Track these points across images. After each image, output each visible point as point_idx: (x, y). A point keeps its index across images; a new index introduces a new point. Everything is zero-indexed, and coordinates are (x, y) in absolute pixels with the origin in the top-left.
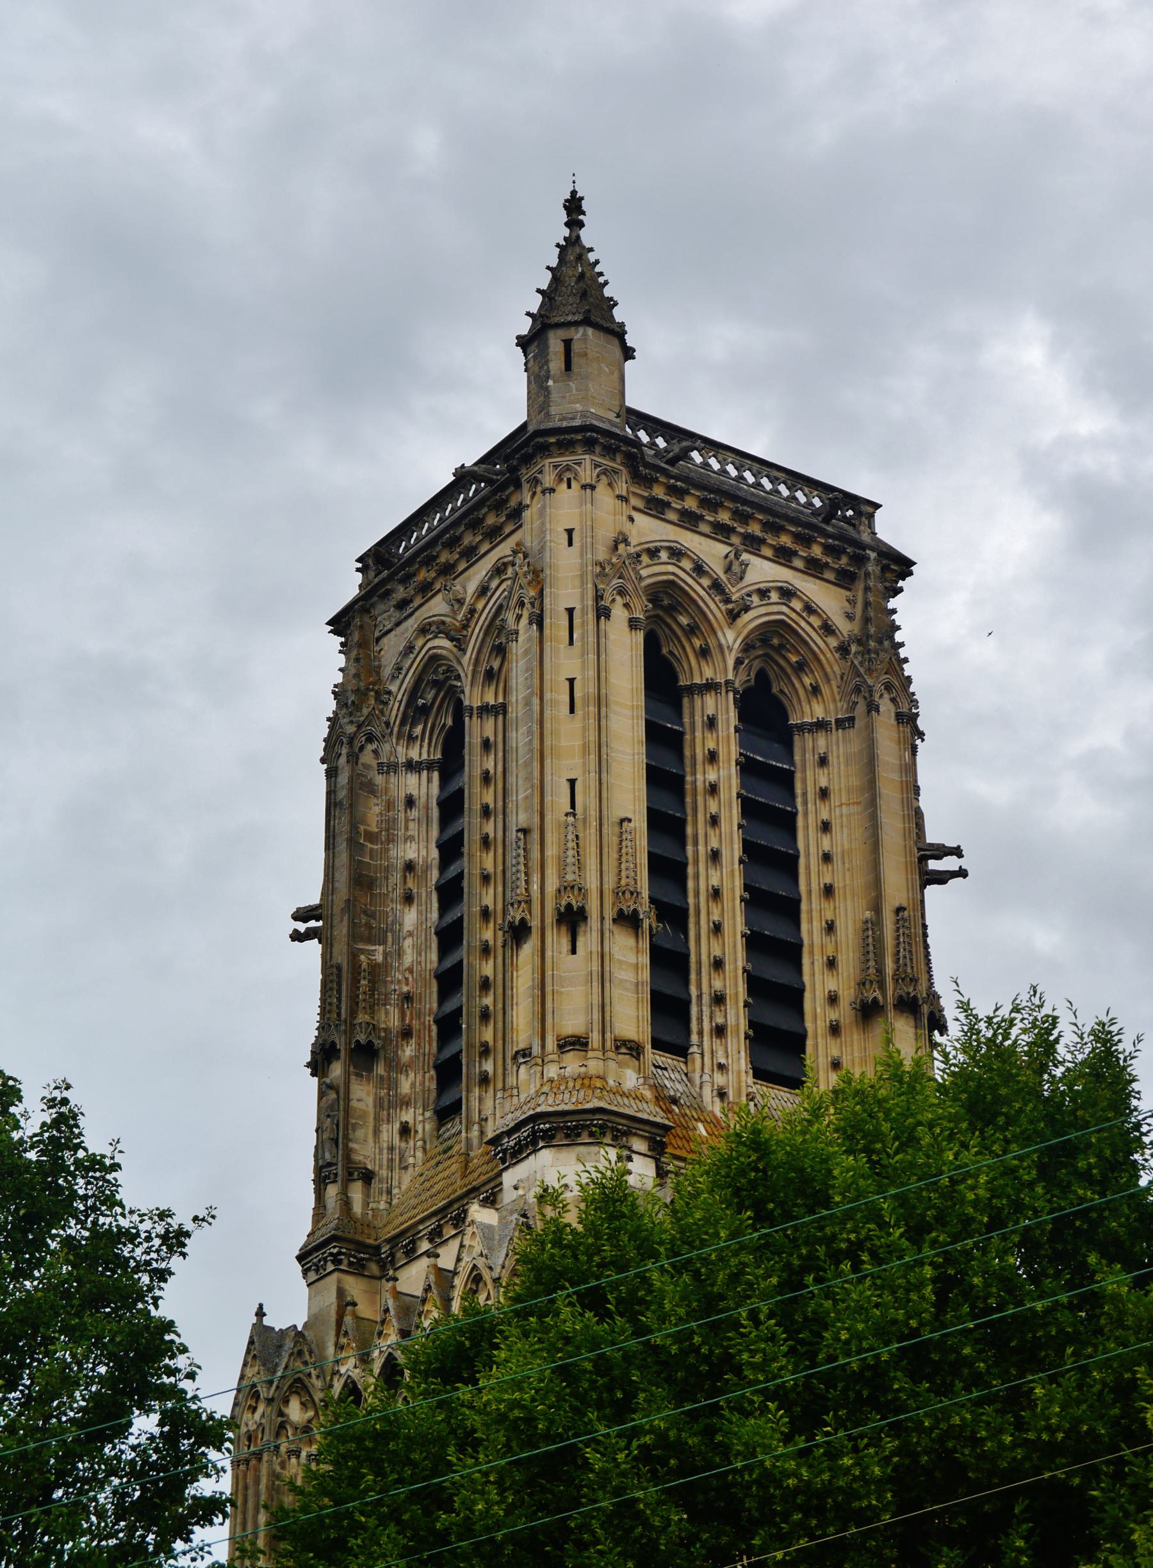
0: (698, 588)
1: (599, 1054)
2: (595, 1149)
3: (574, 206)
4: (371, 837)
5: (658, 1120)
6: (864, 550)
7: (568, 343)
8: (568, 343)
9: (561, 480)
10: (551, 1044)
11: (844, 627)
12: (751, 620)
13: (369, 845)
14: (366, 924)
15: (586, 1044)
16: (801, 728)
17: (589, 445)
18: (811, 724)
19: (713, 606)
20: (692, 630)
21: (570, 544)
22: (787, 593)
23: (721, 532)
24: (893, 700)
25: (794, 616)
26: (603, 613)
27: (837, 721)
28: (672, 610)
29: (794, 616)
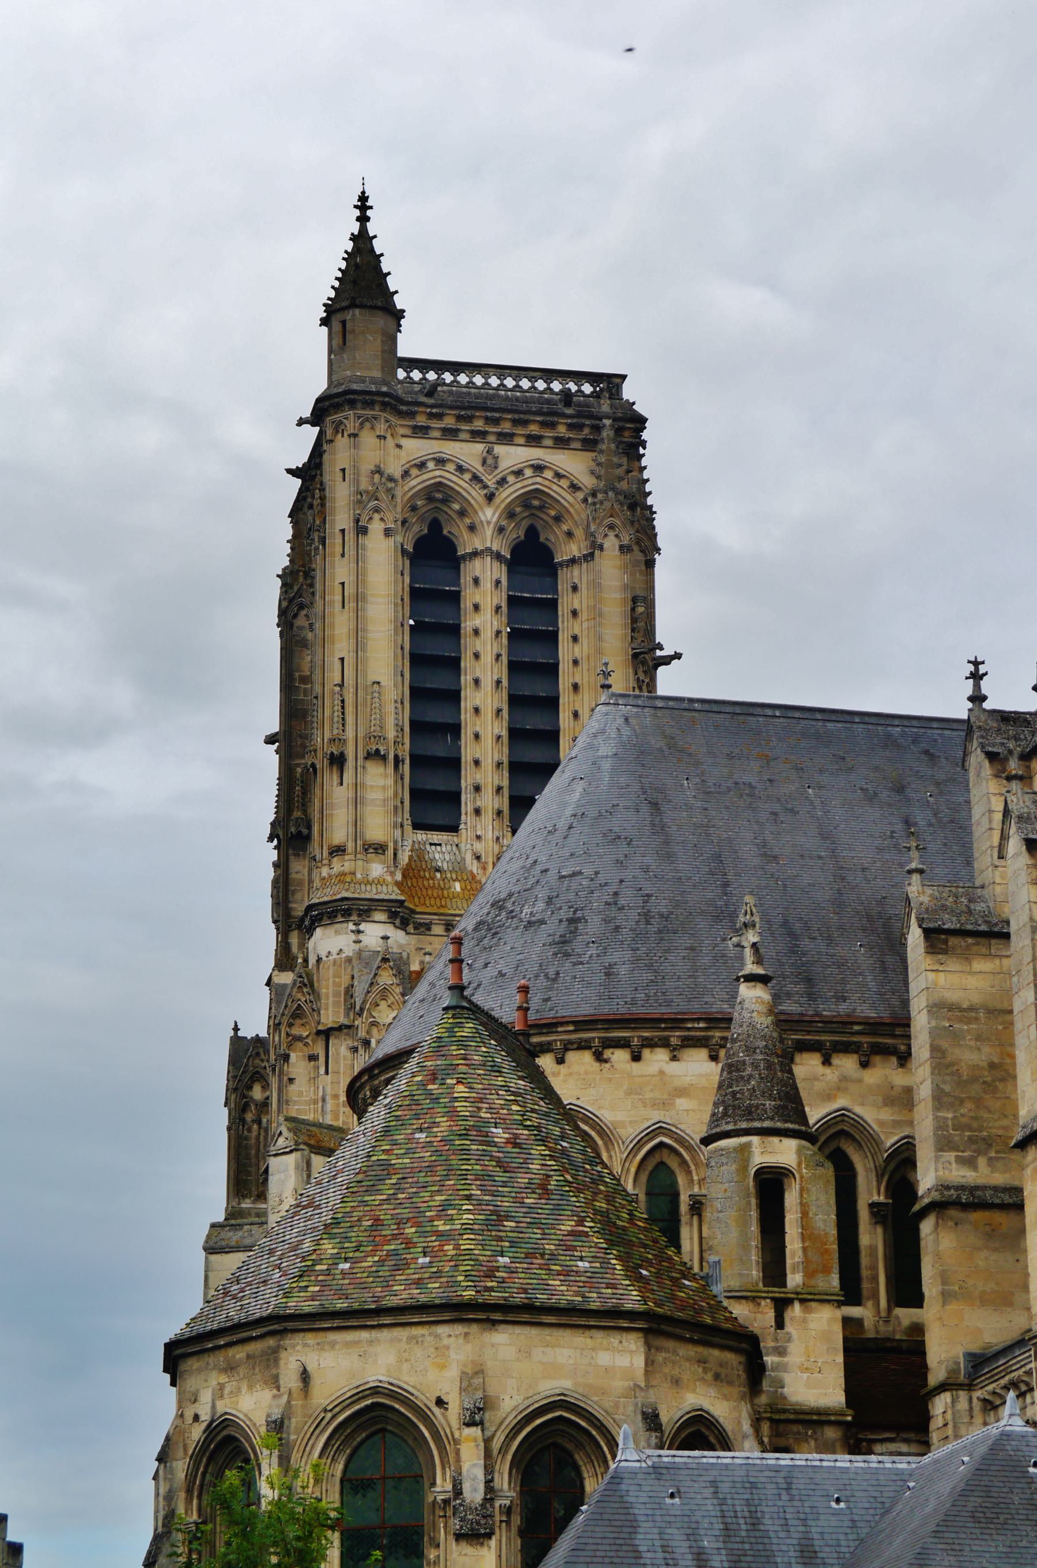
0: (461, 483)
1: (352, 857)
2: (345, 925)
3: (363, 204)
4: (305, 680)
5: (393, 897)
6: (601, 419)
7: (344, 323)
8: (344, 323)
9: (337, 432)
10: (325, 853)
11: (588, 481)
12: (507, 495)
13: (303, 686)
14: (301, 745)
15: (344, 851)
16: (561, 564)
17: (352, 404)
18: (568, 561)
19: (474, 493)
20: (462, 513)
21: (344, 480)
22: (539, 468)
23: (478, 435)
24: (617, 536)
25: (547, 483)
26: (362, 531)
27: (585, 556)
28: (445, 501)
29: (547, 483)
